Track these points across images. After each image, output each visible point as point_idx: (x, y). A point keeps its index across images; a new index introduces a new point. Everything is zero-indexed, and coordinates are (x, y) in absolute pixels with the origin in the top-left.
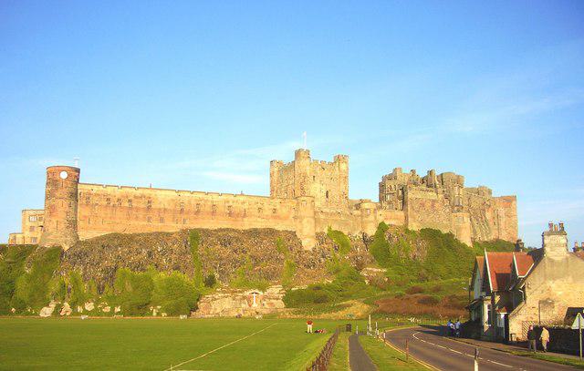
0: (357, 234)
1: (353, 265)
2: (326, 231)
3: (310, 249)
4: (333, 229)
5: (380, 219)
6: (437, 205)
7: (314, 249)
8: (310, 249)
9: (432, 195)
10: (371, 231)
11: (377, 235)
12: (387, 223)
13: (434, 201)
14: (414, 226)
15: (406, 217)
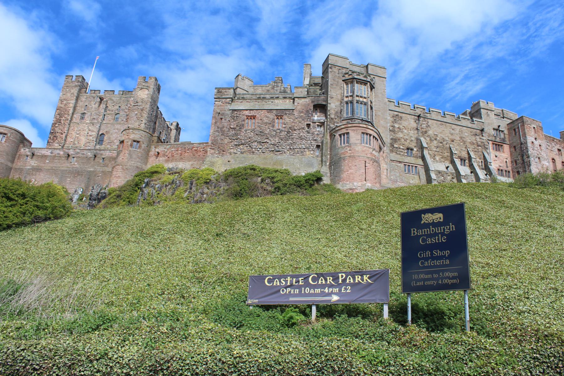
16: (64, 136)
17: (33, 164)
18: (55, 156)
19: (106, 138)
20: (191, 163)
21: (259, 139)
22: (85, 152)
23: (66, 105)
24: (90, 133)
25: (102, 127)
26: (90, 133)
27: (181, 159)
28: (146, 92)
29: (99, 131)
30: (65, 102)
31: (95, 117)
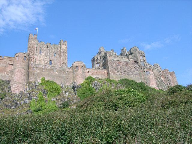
0: (69, 84)
1: (59, 104)
2: (40, 81)
3: (17, 92)
4: (46, 79)
5: (89, 75)
6: (129, 65)
7: (21, 93)
8: (17, 92)
9: (127, 60)
10: (80, 81)
11: (83, 85)
12: (94, 77)
13: (127, 63)
14: (116, 77)
15: (108, 73)
16: (35, 59)
17: (38, 71)
18: (46, 69)
19: (52, 62)
20: (101, 76)
21: (123, 70)
22: (59, 68)
23: (33, 46)
24: (46, 60)
25: (50, 58)
26: (46, 60)
27: (97, 74)
28: (65, 46)
29: (49, 59)
30: (32, 45)
31: (46, 53)
